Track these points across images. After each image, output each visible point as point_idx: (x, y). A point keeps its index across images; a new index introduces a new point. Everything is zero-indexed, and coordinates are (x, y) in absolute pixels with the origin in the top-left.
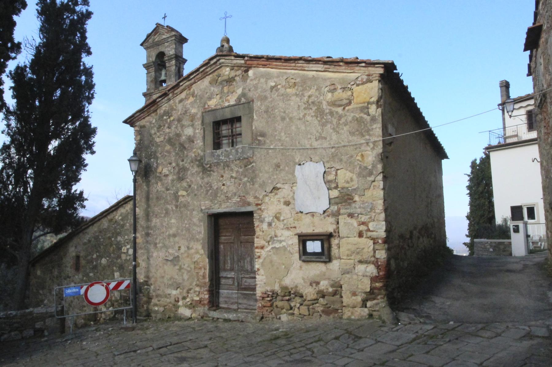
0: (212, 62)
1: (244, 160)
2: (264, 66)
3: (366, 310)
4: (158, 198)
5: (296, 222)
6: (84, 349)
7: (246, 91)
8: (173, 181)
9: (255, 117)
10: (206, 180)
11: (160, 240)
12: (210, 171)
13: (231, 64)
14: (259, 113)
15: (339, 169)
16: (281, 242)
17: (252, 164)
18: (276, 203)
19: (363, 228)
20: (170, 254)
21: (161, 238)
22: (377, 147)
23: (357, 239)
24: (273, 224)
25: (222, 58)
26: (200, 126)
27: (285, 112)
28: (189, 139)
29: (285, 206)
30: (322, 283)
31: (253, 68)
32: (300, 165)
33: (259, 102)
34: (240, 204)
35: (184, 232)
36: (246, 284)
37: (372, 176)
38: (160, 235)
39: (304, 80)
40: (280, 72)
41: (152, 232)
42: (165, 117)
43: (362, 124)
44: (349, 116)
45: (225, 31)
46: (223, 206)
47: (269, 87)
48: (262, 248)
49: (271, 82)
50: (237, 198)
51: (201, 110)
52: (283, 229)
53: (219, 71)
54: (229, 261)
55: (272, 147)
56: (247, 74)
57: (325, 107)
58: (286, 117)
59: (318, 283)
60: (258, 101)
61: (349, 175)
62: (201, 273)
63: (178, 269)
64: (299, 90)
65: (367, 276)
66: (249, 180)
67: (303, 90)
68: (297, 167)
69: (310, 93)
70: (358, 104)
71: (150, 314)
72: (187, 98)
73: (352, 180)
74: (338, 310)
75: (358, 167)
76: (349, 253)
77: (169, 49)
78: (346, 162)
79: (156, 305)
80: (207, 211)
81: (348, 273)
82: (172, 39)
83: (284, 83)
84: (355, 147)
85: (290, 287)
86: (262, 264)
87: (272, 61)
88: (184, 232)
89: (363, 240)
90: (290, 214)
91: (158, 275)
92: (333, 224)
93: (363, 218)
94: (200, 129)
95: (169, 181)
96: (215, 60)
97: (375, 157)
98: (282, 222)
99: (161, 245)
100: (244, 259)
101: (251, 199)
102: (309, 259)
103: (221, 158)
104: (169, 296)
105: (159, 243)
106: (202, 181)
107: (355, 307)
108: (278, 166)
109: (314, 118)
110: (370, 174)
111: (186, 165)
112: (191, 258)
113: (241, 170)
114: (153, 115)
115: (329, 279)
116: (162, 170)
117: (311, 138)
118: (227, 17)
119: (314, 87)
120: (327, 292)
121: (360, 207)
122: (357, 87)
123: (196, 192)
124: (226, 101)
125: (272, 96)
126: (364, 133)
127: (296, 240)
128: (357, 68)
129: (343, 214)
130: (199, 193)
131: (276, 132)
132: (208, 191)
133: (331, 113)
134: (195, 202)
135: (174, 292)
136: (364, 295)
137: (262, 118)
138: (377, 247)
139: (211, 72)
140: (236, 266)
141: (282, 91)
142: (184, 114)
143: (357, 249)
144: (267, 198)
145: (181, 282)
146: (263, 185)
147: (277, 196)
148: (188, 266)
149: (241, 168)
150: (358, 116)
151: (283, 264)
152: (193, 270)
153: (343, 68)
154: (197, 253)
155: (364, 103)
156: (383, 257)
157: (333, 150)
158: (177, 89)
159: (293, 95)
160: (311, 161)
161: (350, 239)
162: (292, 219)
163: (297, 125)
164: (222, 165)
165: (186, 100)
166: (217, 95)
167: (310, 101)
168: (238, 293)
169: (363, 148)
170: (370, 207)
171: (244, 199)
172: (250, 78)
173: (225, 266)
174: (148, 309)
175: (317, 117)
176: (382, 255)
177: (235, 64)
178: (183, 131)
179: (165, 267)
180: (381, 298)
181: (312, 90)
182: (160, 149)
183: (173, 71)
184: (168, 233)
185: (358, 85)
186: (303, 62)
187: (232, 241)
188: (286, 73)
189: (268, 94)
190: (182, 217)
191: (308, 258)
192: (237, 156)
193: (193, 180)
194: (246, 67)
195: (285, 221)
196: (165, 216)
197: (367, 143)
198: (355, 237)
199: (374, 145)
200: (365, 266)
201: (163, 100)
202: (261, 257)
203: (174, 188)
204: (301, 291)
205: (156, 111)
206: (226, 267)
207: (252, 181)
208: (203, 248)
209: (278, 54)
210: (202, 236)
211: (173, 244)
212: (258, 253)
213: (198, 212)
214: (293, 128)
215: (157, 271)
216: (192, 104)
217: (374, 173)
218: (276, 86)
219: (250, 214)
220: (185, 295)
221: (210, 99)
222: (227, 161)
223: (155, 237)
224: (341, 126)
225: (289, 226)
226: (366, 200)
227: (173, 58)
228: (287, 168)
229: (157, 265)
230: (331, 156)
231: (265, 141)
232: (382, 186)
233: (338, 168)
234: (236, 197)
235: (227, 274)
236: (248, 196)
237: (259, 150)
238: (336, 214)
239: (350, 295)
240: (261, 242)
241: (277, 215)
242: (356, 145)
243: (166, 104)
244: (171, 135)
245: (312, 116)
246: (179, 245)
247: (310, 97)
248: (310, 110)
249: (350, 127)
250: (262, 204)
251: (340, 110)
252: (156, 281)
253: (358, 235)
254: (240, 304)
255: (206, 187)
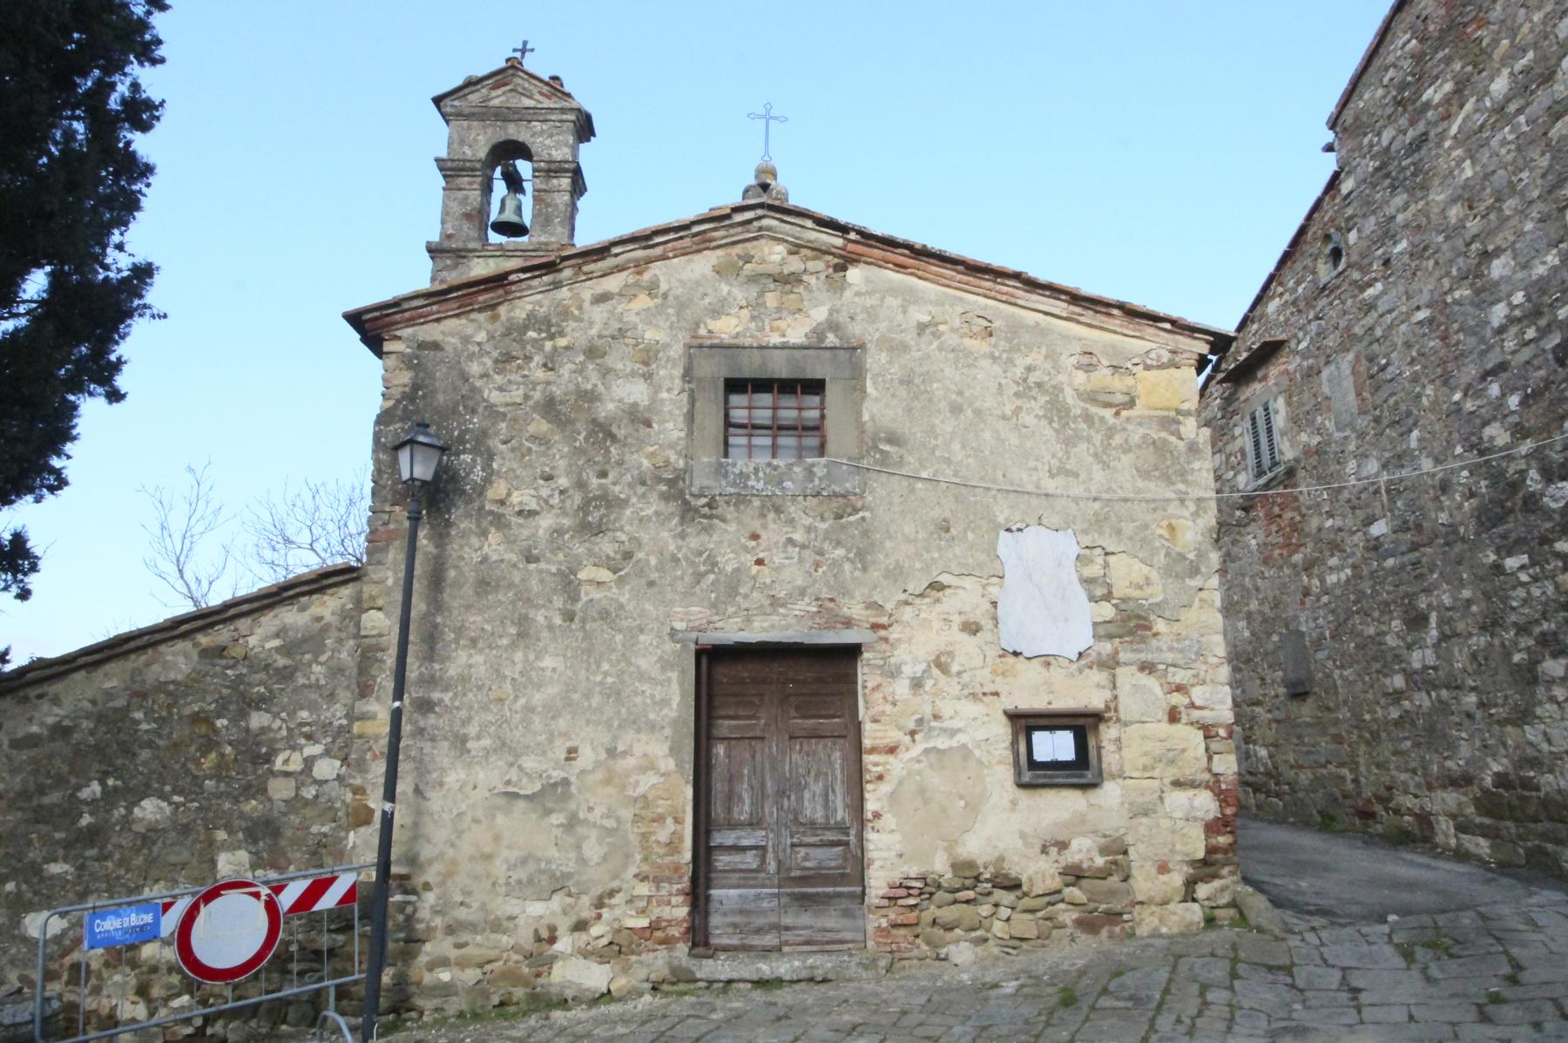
0: (738, 218)
2: (900, 267)
3: (1196, 906)
4: (484, 585)
5: (999, 679)
7: (842, 318)
8: (559, 531)
9: (870, 389)
10: (694, 542)
11: (484, 727)
12: (710, 517)
13: (797, 238)
15: (1113, 553)
16: (953, 732)
17: (861, 514)
18: (936, 625)
19: (1178, 699)
21: (490, 718)
22: (1205, 512)
23: (1165, 727)
24: (929, 684)
25: (772, 214)
27: (960, 393)
28: (631, 413)
29: (965, 636)
30: (1075, 844)
31: (862, 265)
32: (1008, 530)
34: (817, 620)
35: (596, 700)
36: (807, 864)
38: (485, 708)
39: (1015, 328)
40: (944, 293)
41: (447, 697)
42: (532, 334)
44: (1133, 431)
46: (756, 624)
48: (892, 750)
50: (809, 604)
51: (683, 338)
52: (960, 699)
53: (748, 245)
55: (924, 475)
56: (842, 274)
57: (1070, 401)
58: (965, 406)
59: (1063, 846)
61: (1138, 570)
62: (663, 835)
65: (1196, 819)
66: (852, 555)
67: (1011, 350)
68: (1003, 534)
69: (1028, 361)
71: (407, 998)
72: (627, 294)
74: (1120, 914)
77: (548, 142)
78: (1131, 539)
79: (444, 962)
80: (694, 635)
81: (1146, 815)
82: (564, 117)
83: (957, 323)
84: (1153, 506)
85: (980, 862)
86: (893, 797)
87: (931, 261)
89: (1180, 729)
91: (466, 848)
92: (1104, 687)
93: (1180, 676)
94: (676, 392)
95: (541, 532)
96: (749, 215)
97: (1202, 534)
98: (956, 679)
99: (486, 742)
100: (800, 788)
101: (855, 610)
102: (1041, 781)
103: (750, 483)
104: (511, 925)
105: (479, 737)
106: (680, 543)
107: (1167, 903)
109: (1044, 422)
110: (1194, 571)
111: (617, 489)
112: (623, 787)
113: (823, 526)
114: (481, 317)
115: (1095, 832)
116: (509, 495)
121: (1171, 649)
123: (655, 576)
124: (772, 330)
125: (923, 347)
127: (1001, 730)
128: (1151, 331)
129: (1126, 664)
131: (936, 438)
132: (699, 577)
133: (1088, 418)
134: (649, 607)
135: (536, 909)
137: (893, 396)
138: (1214, 746)
139: (723, 242)
140: (770, 812)
141: (953, 340)
142: (613, 337)
143: (1169, 750)
144: (908, 609)
145: (571, 867)
146: (896, 574)
147: (938, 608)
149: (823, 519)
150: (1156, 437)
151: (962, 797)
152: (628, 826)
153: (1117, 322)
154: (649, 766)
155: (1167, 409)
156: (1230, 772)
157: (1097, 505)
159: (984, 356)
162: (987, 671)
163: (997, 431)
164: (757, 503)
165: (623, 299)
166: (741, 308)
167: (1032, 379)
168: (777, 896)
171: (832, 609)
172: (856, 288)
173: (729, 810)
174: (401, 982)
175: (1051, 422)
176: (1227, 765)
179: (500, 819)
180: (1232, 873)
181: (1033, 355)
182: (504, 425)
183: (562, 207)
184: (522, 701)
185: (1148, 368)
186: (1019, 285)
187: (758, 733)
188: (961, 299)
189: (910, 337)
190: (588, 651)
193: (645, 537)
194: (841, 257)
195: (966, 678)
196: (513, 645)
197: (1182, 501)
200: (1191, 792)
201: (535, 282)
202: (887, 778)
203: (561, 556)
205: (493, 307)
206: (736, 816)
207: (862, 558)
208: (674, 751)
212: (876, 765)
214: (987, 435)
215: (459, 837)
216: (649, 316)
217: (1203, 569)
218: (934, 323)
219: (851, 652)
220: (587, 914)
221: (716, 312)
222: (774, 494)
223: (463, 714)
225: (979, 690)
227: (566, 171)
228: (970, 536)
229: (460, 815)
230: (1093, 519)
232: (1218, 603)
233: (1109, 549)
235: (739, 838)
239: (1154, 871)
240: (890, 734)
241: (943, 659)
242: (1154, 501)
243: (539, 297)
244: (557, 392)
245: (1036, 416)
246: (568, 744)
247: (1029, 369)
249: (1138, 458)
250: (890, 625)
251: (1108, 414)
252: (449, 875)
253: (1166, 717)
254: (787, 928)
255: (692, 564)
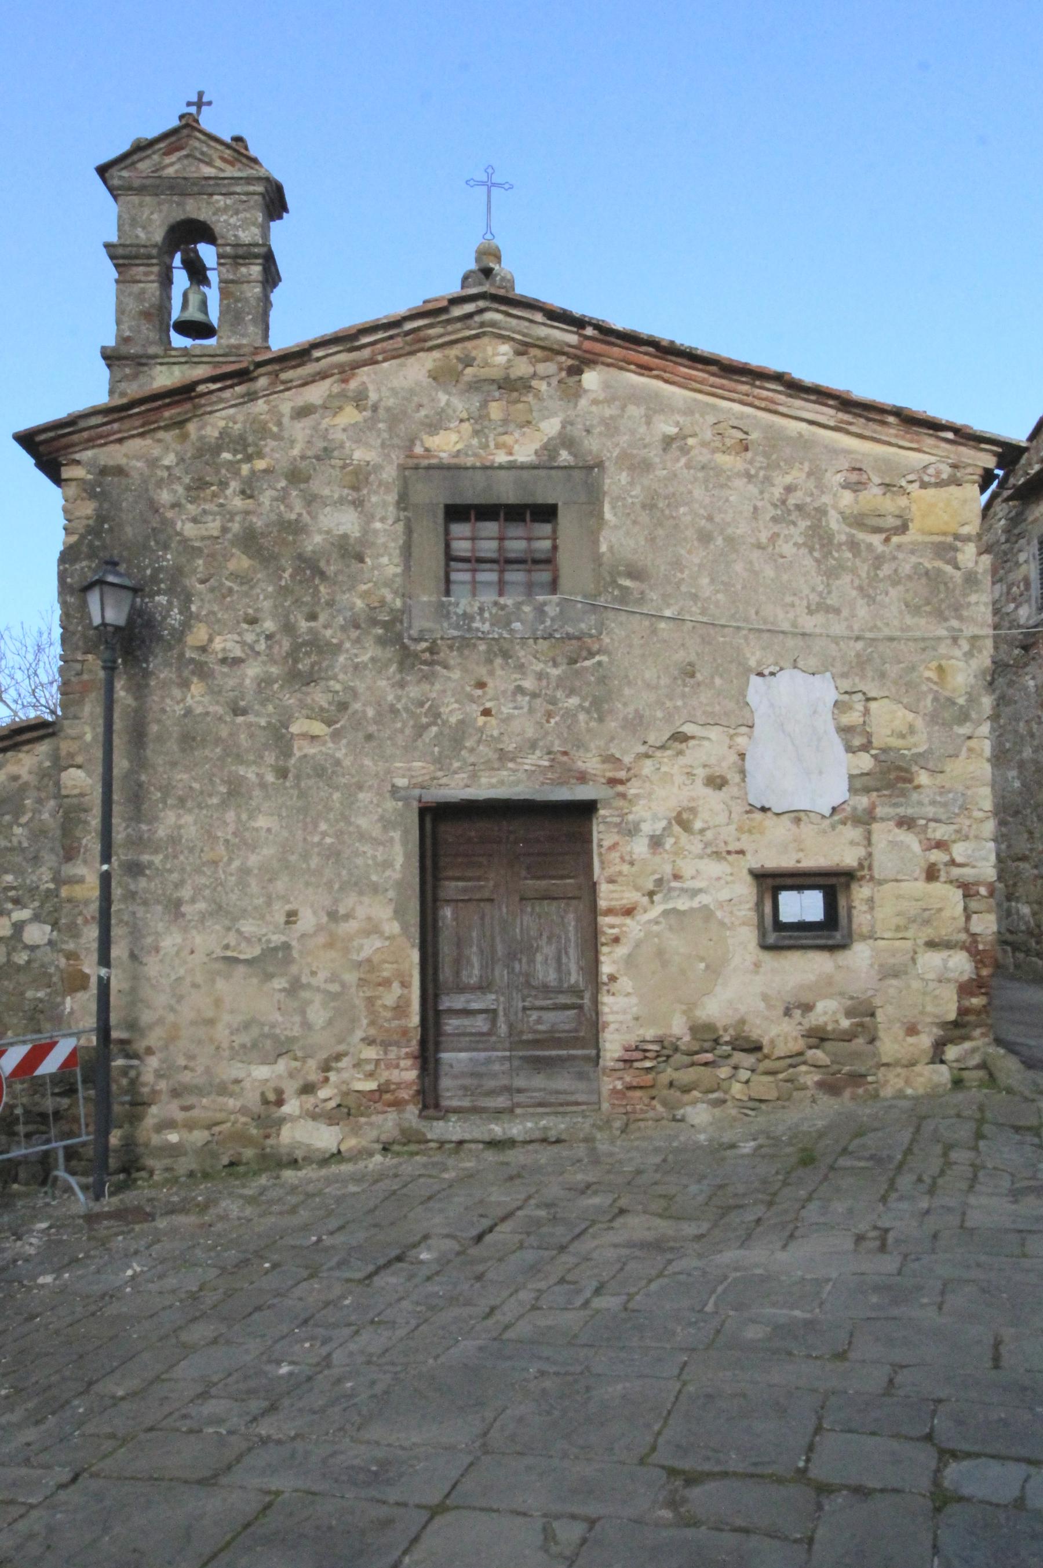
0: (457, 311)
1: (567, 642)
2: (644, 369)
3: (943, 1068)
4: (188, 740)
5: (745, 837)
6: (665, 1196)
7: (577, 431)
8: (265, 682)
9: (608, 515)
10: (414, 691)
11: (198, 890)
12: (431, 663)
13: (524, 335)
14: (624, 506)
15: (875, 699)
16: (694, 893)
17: (597, 658)
18: (679, 779)
19: (937, 856)
20: (248, 940)
21: (203, 880)
22: (980, 651)
23: (921, 886)
24: (669, 842)
25: (495, 306)
26: (391, 509)
27: (710, 518)
28: (341, 547)
29: (709, 791)
30: (820, 1006)
31: (600, 367)
32: (760, 674)
33: (624, 474)
34: (550, 775)
35: (314, 862)
36: (540, 1027)
37: (968, 724)
38: (198, 871)
39: (774, 440)
40: (695, 400)
41: (157, 859)
42: (226, 456)
43: (942, 587)
44: (904, 560)
45: (489, 226)
46: (484, 780)
47: (658, 437)
48: (629, 912)
49: (665, 422)
50: (541, 758)
51: (397, 457)
52: (701, 857)
53: (469, 345)
54: (475, 960)
55: (668, 613)
56: (577, 378)
57: (834, 525)
58: (716, 534)
59: (807, 1008)
60: (622, 470)
61: (902, 717)
62: (390, 997)
63: (284, 990)
64: (758, 465)
65: (949, 980)
66: (587, 704)
67: (768, 467)
68: (754, 679)
69: (788, 479)
70: (923, 532)
71: (137, 1159)
72: (331, 406)
73: (912, 730)
74: (865, 1076)
75: (930, 697)
76: (901, 921)
77: (232, 221)
78: (895, 683)
79: (169, 1124)
80: (417, 792)
81: (896, 975)
82: (251, 188)
83: (708, 435)
84: (922, 645)
85: (720, 1025)
86: (630, 961)
87: (679, 360)
88: (314, 862)
89: (938, 888)
90: (727, 813)
91: (186, 1013)
92: (858, 844)
93: (940, 832)
94: (390, 522)
95: (248, 681)
96: (469, 308)
97: (975, 676)
98: (699, 837)
99: (201, 906)
100: (531, 951)
101: (590, 763)
102: (787, 942)
103: (475, 625)
104: (236, 1088)
105: (193, 900)
106: (399, 692)
107: (913, 1065)
108: (689, 672)
109: (804, 551)
110: (963, 717)
111: (328, 633)
112: (346, 950)
113: (555, 672)
114: (167, 436)
115: (842, 994)
116: (211, 640)
117: (793, 605)
118: (494, 185)
119: (801, 463)
120: (834, 1030)
121: (933, 803)
122: (923, 491)
123: (372, 729)
124: (498, 446)
125: (669, 464)
126: (947, 613)
127: (745, 890)
128: (931, 441)
129: (883, 819)
130: (388, 733)
131: (682, 572)
132: (420, 730)
133: (853, 545)
134: (367, 762)
135: (261, 1072)
136: (938, 1032)
137: (635, 522)
138: (974, 905)
139: (440, 341)
140: (501, 975)
141: (702, 456)
142: (318, 458)
143: (925, 910)
144: (648, 762)
145: (296, 1031)
146: (636, 724)
147: (682, 760)
148: (333, 978)
149: (555, 665)
150: (929, 566)
151: (702, 959)
152: (353, 990)
153: (892, 431)
154: (373, 929)
155: (945, 534)
156: (989, 931)
157: (860, 645)
158: (294, 367)
159: (738, 475)
160: (795, 667)
161: (903, 884)
162: (732, 828)
163: (751, 562)
164: (482, 647)
165: (328, 413)
166: (462, 421)
167: (791, 501)
168: (510, 1059)
169: (943, 650)
170: (959, 803)
171: (565, 763)
172: (592, 396)
173: (457, 973)
174: (129, 1144)
175: (811, 550)
176: (986, 925)
177: (539, 339)
178: (314, 518)
179: (221, 984)
180: (983, 1035)
181: (795, 473)
182: (200, 562)
183: (253, 302)
184: (236, 864)
185: (924, 485)
186: (780, 388)
187: (486, 894)
188: (714, 407)
189: (654, 454)
190: (304, 810)
191: (790, 937)
192: (542, 627)
193: (360, 686)
194: (575, 357)
195: (709, 835)
196: (224, 804)
197: (955, 640)
198: (916, 879)
199: (973, 646)
200: (945, 954)
201: (227, 394)
202: (623, 940)
203: (270, 708)
204: (755, 1034)
205: (181, 424)
206: (465, 979)
207: (599, 707)
208: (399, 913)
209: (705, 345)
210: (395, 873)
211: (261, 901)
212: (612, 927)
213: (379, 794)
214: (739, 567)
215: (178, 1002)
216: (358, 433)
217: (974, 715)
218: (682, 436)
219: (587, 809)
220: (314, 1077)
221: (434, 426)
222: (501, 637)
223: (175, 876)
224: (881, 585)
225: (723, 848)
226: (948, 785)
227: (256, 256)
228: (718, 681)
229: (179, 980)
230: (855, 660)
231: (642, 593)
232: (987, 751)
233: (871, 695)
234: (538, 753)
235: (468, 1002)
236: (581, 753)
237: (623, 617)
238: (865, 819)
239: (901, 1033)
240: (626, 895)
241: (685, 816)
242: (924, 639)
243: (232, 411)
244: (259, 523)
245: (795, 544)
246: (288, 907)
247: (789, 489)
248: (792, 527)
249: (907, 591)
250: (629, 780)
251: (876, 540)
252: (172, 1038)
253: (924, 875)
254: (519, 1091)
255: (412, 715)
